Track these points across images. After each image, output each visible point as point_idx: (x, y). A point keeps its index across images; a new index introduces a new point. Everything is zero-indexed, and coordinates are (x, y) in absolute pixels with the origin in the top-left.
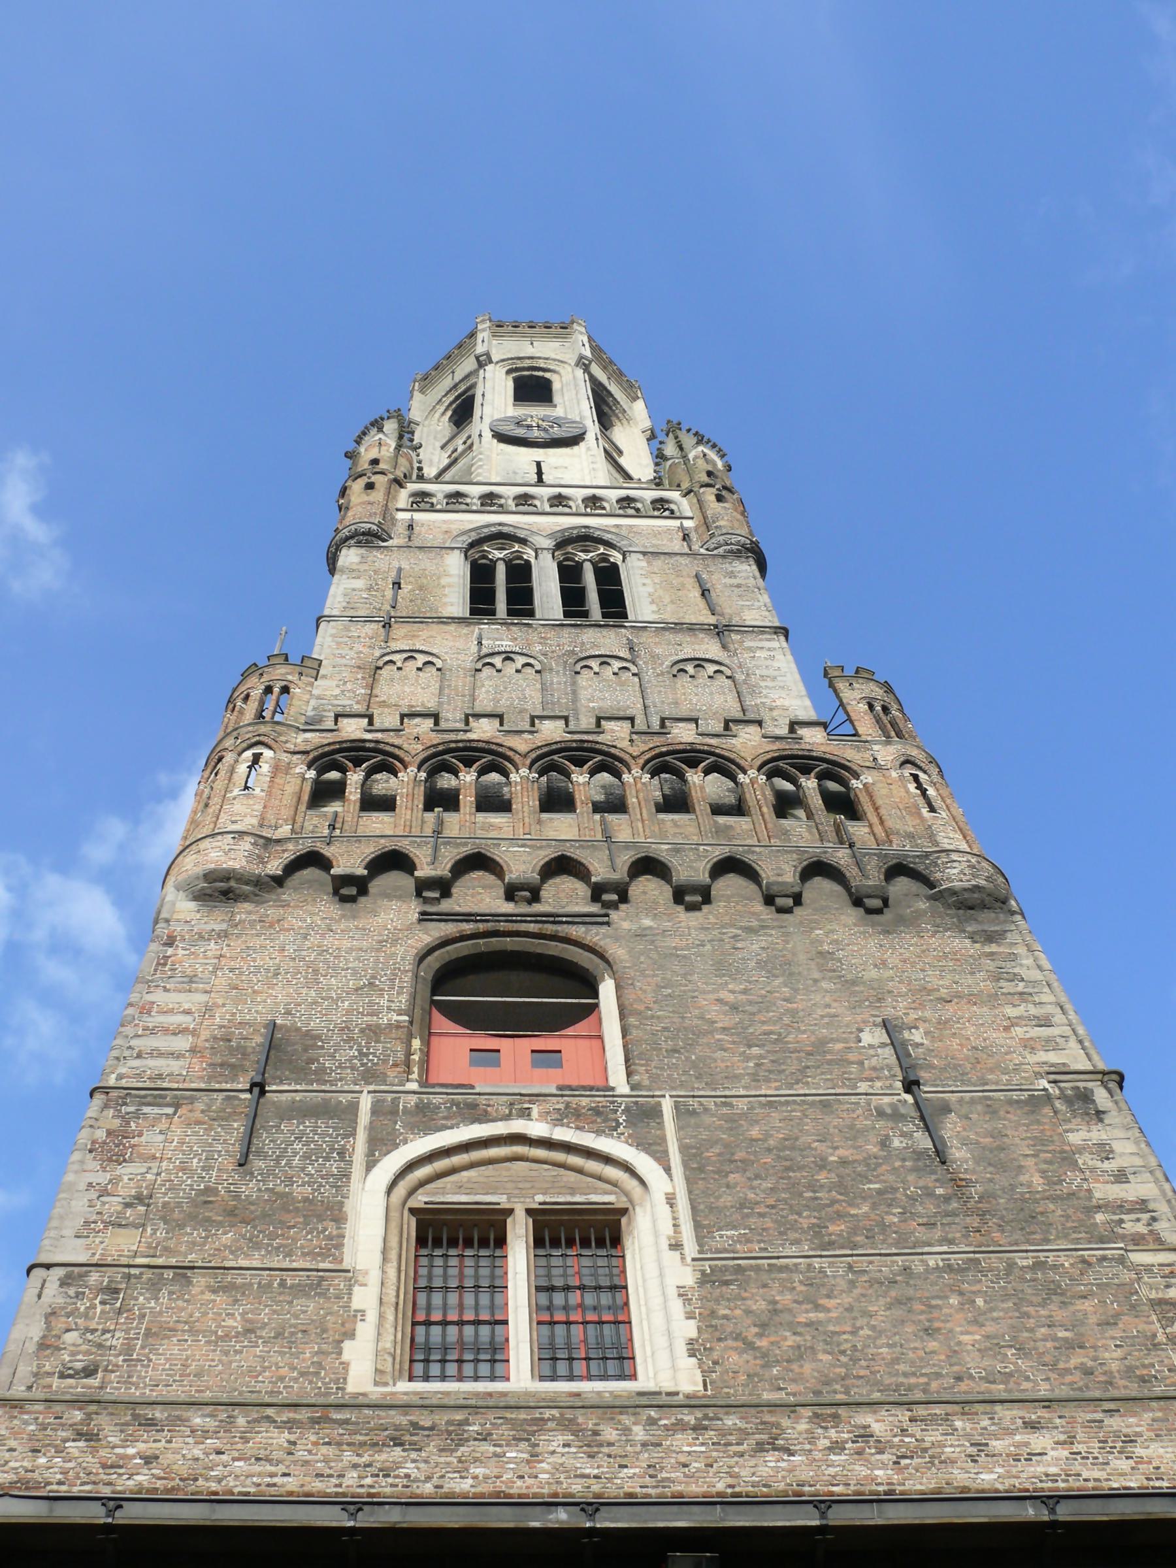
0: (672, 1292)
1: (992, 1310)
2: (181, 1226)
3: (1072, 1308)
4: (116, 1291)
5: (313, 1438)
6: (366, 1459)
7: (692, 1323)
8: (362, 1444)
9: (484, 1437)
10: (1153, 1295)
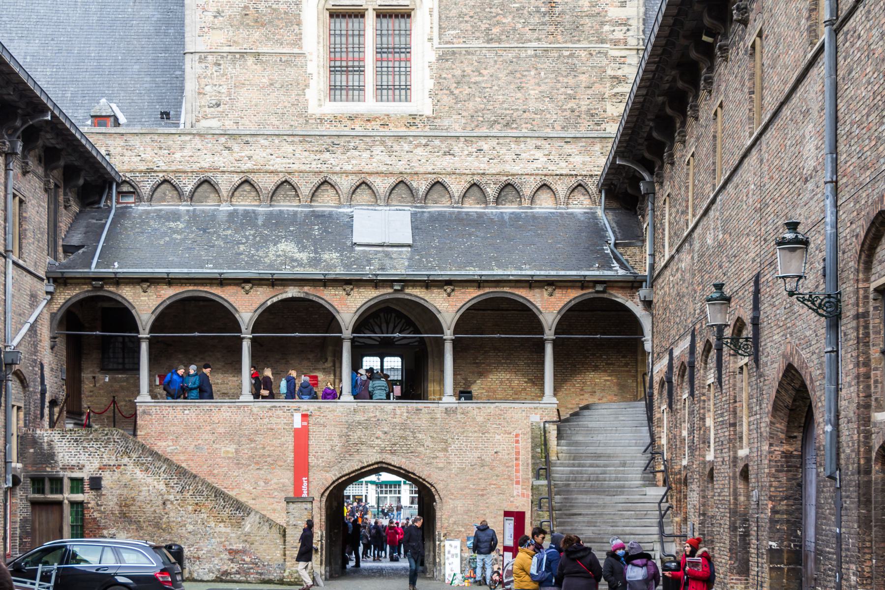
0: (427, 65)
1: (546, 78)
2: (238, 29)
3: (577, 79)
4: (219, 65)
5: (301, 148)
6: (317, 158)
7: (432, 81)
8: (317, 151)
9: (355, 148)
10: (612, 73)
